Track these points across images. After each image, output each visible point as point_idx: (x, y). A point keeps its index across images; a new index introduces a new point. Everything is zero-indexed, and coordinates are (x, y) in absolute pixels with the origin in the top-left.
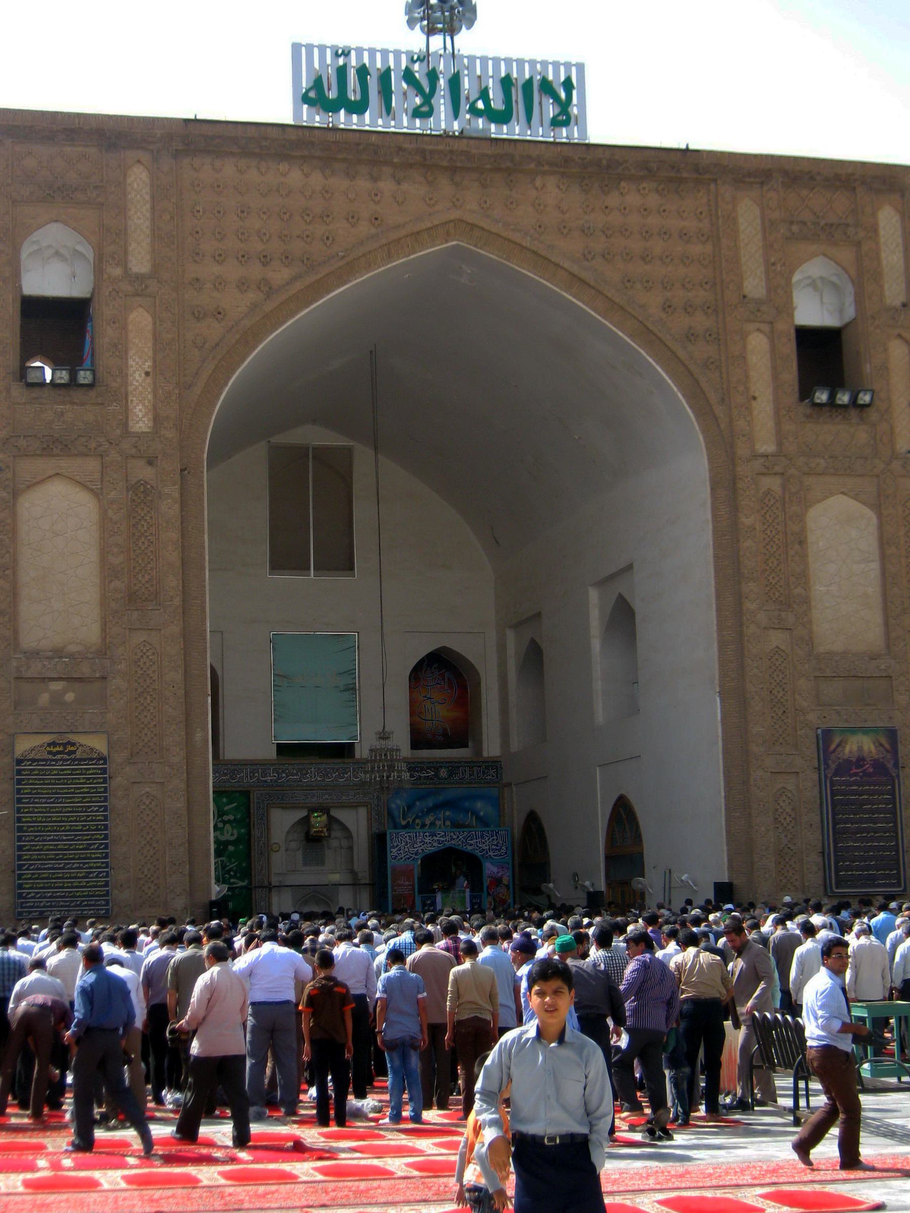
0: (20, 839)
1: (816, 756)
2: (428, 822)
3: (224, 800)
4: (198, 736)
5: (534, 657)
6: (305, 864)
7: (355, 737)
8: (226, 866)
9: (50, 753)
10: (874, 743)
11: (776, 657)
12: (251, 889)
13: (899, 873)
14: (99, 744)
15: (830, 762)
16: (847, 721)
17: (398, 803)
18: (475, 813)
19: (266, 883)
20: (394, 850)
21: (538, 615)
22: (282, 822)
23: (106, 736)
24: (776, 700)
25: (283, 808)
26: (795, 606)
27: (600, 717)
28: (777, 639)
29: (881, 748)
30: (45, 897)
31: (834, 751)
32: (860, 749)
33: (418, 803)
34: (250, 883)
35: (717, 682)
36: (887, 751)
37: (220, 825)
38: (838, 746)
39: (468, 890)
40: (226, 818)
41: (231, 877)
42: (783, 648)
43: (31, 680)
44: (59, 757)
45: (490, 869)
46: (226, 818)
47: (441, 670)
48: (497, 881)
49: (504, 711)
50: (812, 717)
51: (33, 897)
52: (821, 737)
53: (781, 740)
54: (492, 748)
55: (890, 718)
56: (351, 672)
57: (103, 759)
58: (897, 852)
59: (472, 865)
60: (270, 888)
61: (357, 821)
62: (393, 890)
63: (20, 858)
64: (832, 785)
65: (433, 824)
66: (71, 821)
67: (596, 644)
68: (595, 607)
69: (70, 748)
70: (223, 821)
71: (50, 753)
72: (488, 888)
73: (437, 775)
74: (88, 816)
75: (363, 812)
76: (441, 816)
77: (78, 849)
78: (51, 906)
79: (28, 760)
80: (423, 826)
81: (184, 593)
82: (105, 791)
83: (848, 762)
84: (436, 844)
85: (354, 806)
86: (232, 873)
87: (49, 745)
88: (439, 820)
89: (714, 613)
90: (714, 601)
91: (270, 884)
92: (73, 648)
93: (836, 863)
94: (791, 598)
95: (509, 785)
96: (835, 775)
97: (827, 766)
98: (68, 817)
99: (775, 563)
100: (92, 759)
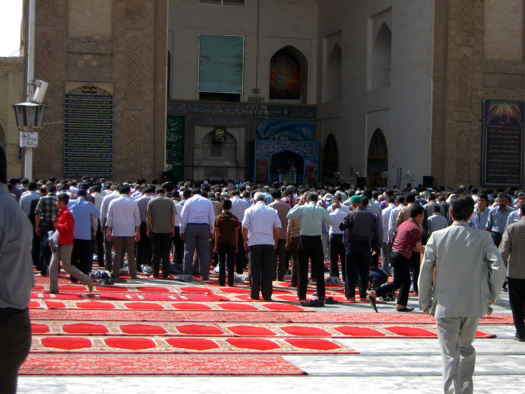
0: (66, 136)
1: (481, 114)
2: (276, 137)
4: (160, 86)
5: (336, 54)
6: (211, 156)
7: (241, 91)
9: (83, 92)
10: (512, 109)
12: (183, 167)
13: (519, 177)
14: (108, 88)
15: (488, 117)
16: (498, 96)
17: (262, 126)
18: (301, 134)
19: (191, 165)
20: (258, 151)
21: (340, 32)
22: (201, 133)
23: (112, 84)
27: (370, 86)
28: (465, 51)
29: (515, 112)
30: (79, 166)
31: (491, 112)
32: (504, 111)
33: (272, 127)
34: (183, 164)
35: (432, 72)
36: (518, 113)
37: (169, 133)
38: (493, 108)
39: (295, 173)
40: (172, 130)
41: (173, 160)
42: (468, 56)
43: (74, 53)
44: (88, 94)
45: (307, 163)
46: (172, 130)
47: (288, 58)
48: (311, 170)
49: (319, 82)
50: (480, 93)
51: (72, 166)
52: (484, 104)
53: (463, 104)
54: (312, 100)
55: (521, 96)
56: (240, 57)
57: (111, 96)
58: (520, 166)
59: (298, 160)
60: (193, 167)
61: (240, 135)
62: (257, 171)
63: (66, 145)
64: (488, 129)
65: (279, 138)
66: (93, 128)
67: (370, 49)
68: (371, 29)
69: (94, 90)
70: (171, 132)
71: (83, 92)
72: (306, 173)
73: (282, 113)
74: (102, 126)
75: (243, 130)
76: (283, 134)
77: (97, 142)
78: (82, 171)
79: (72, 95)
80: (274, 139)
81: (155, 11)
82: (111, 113)
83: (498, 118)
84: (280, 149)
85: (239, 127)
87: (83, 88)
88: (283, 136)
89: (433, 36)
90: (433, 29)
91: (193, 165)
92: (96, 38)
93: (487, 169)
94: (474, 30)
95: (320, 120)
96: (490, 124)
97: (486, 119)
98: (92, 125)
99: (467, 11)
100: (105, 96)
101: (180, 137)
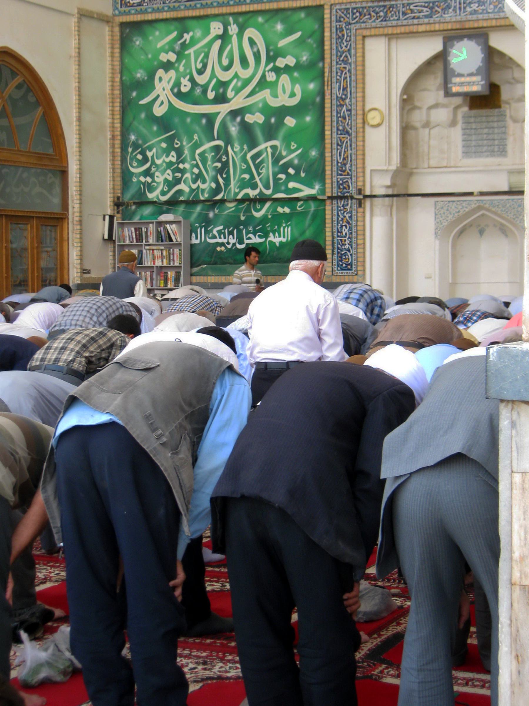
3: (279, 27)
8: (281, 157)
25: (390, 37)
37: (271, 77)
40: (281, 63)
46: (281, 63)
60: (363, 198)
70: (277, 70)
86: (291, 171)
91: (360, 191)
101: (312, 86)
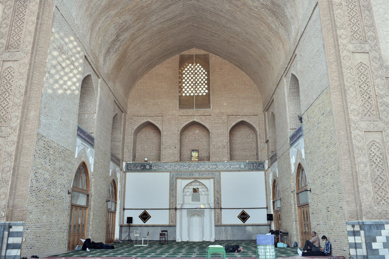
11: (361, 68)
24: (364, 91)
26: (369, 41)
